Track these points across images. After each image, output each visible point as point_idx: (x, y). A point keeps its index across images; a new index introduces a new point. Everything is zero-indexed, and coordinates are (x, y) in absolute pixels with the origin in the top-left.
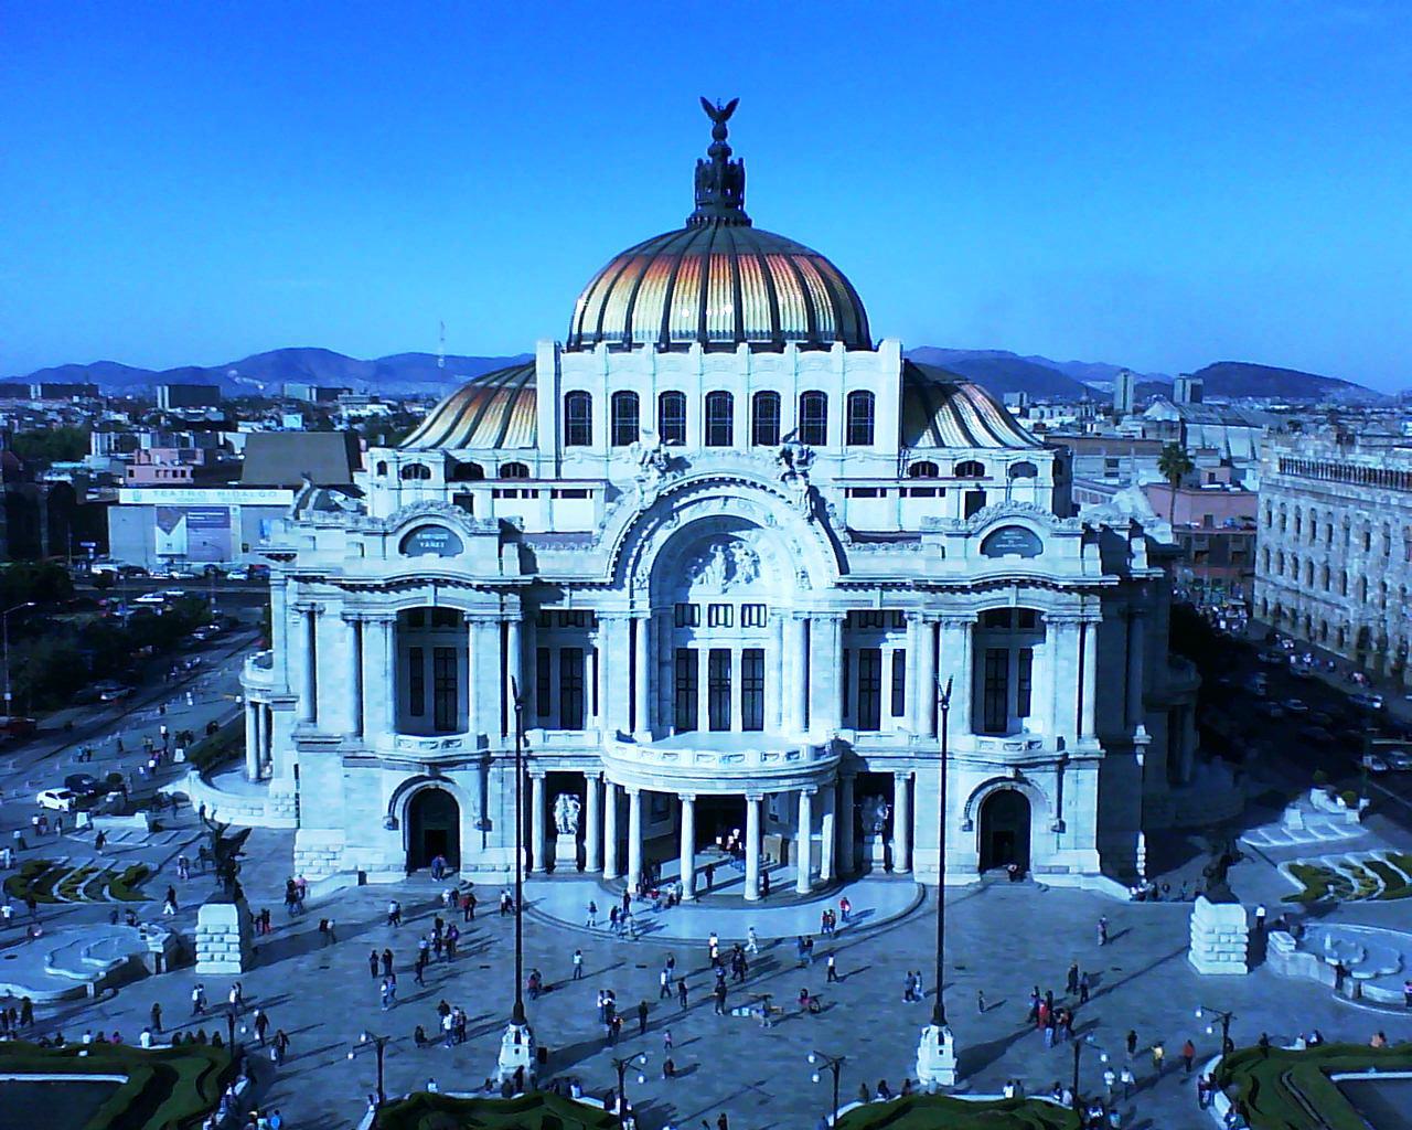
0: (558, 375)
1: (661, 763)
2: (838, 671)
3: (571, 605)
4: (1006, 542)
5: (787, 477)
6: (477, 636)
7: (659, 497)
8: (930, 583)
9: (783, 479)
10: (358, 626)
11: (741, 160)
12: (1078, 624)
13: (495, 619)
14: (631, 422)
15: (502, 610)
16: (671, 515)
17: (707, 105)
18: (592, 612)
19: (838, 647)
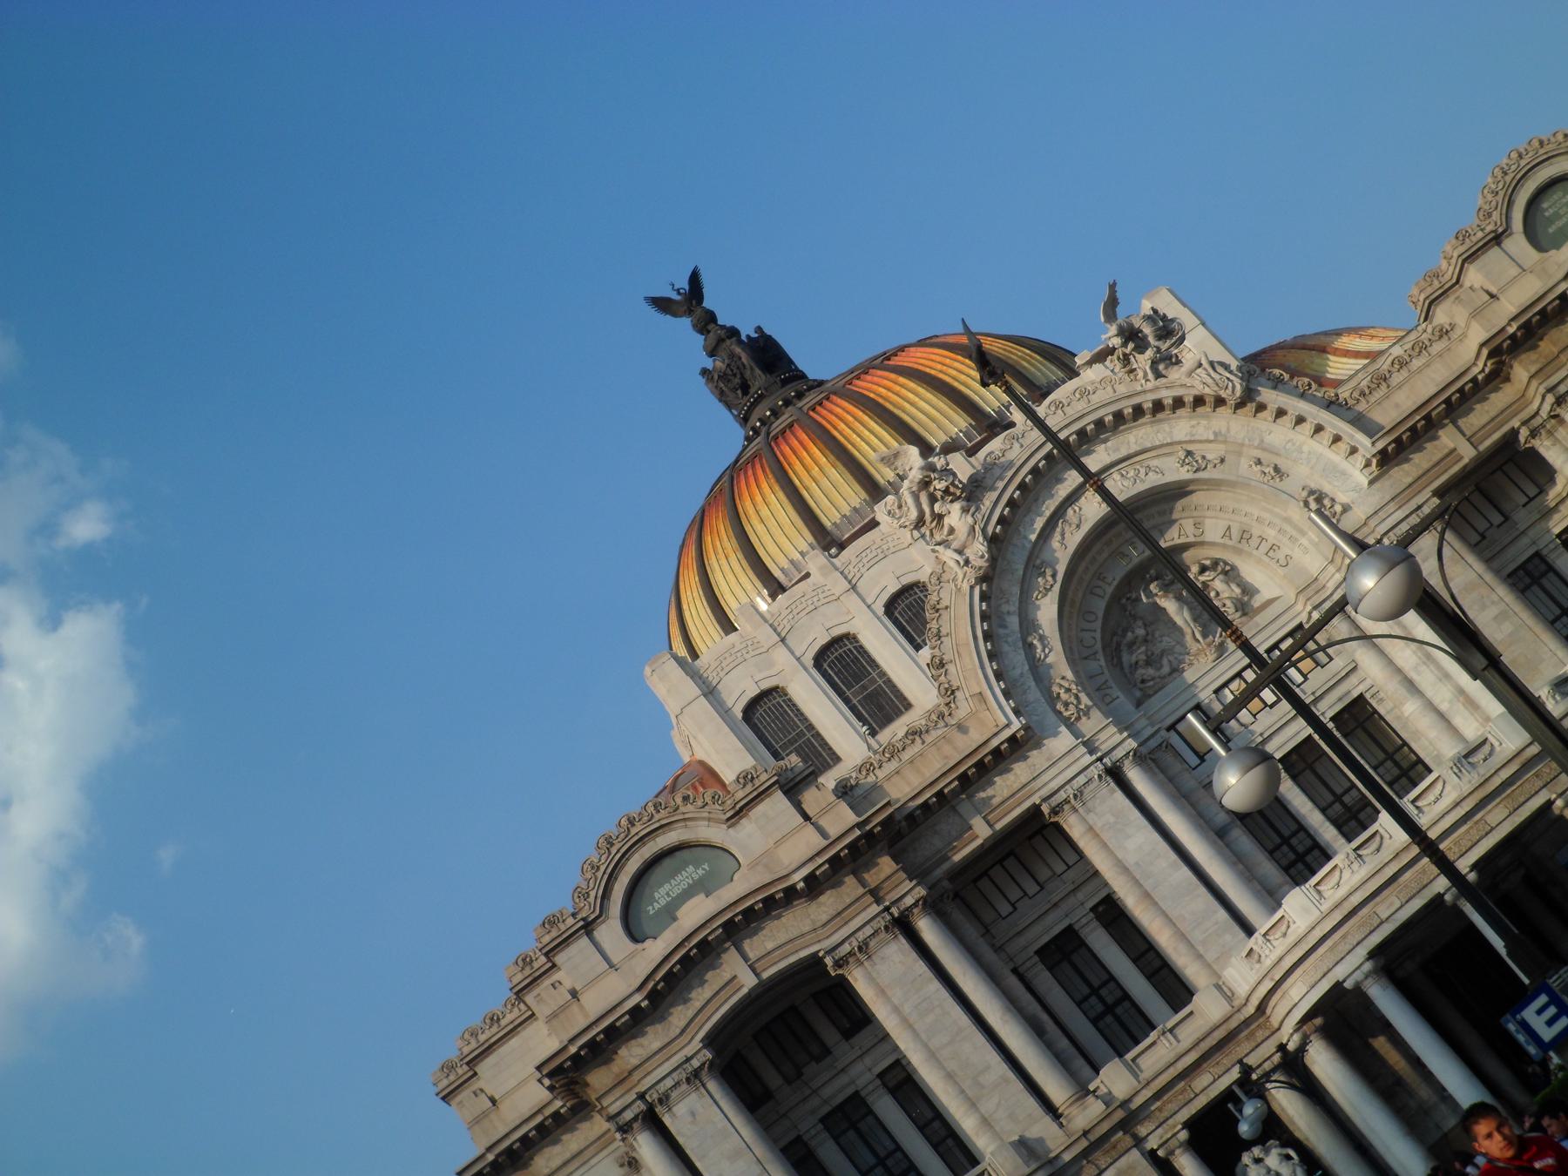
0: (710, 692)
1: (1362, 872)
2: (1502, 591)
4: (1557, 216)
5: (1161, 367)
6: (871, 979)
7: (993, 541)
8: (1511, 330)
9: (1158, 375)
10: (653, 1121)
11: (759, 329)
13: (880, 923)
14: (873, 681)
15: (878, 901)
16: (1036, 563)
17: (662, 305)
18: (1035, 811)
19: (1471, 559)
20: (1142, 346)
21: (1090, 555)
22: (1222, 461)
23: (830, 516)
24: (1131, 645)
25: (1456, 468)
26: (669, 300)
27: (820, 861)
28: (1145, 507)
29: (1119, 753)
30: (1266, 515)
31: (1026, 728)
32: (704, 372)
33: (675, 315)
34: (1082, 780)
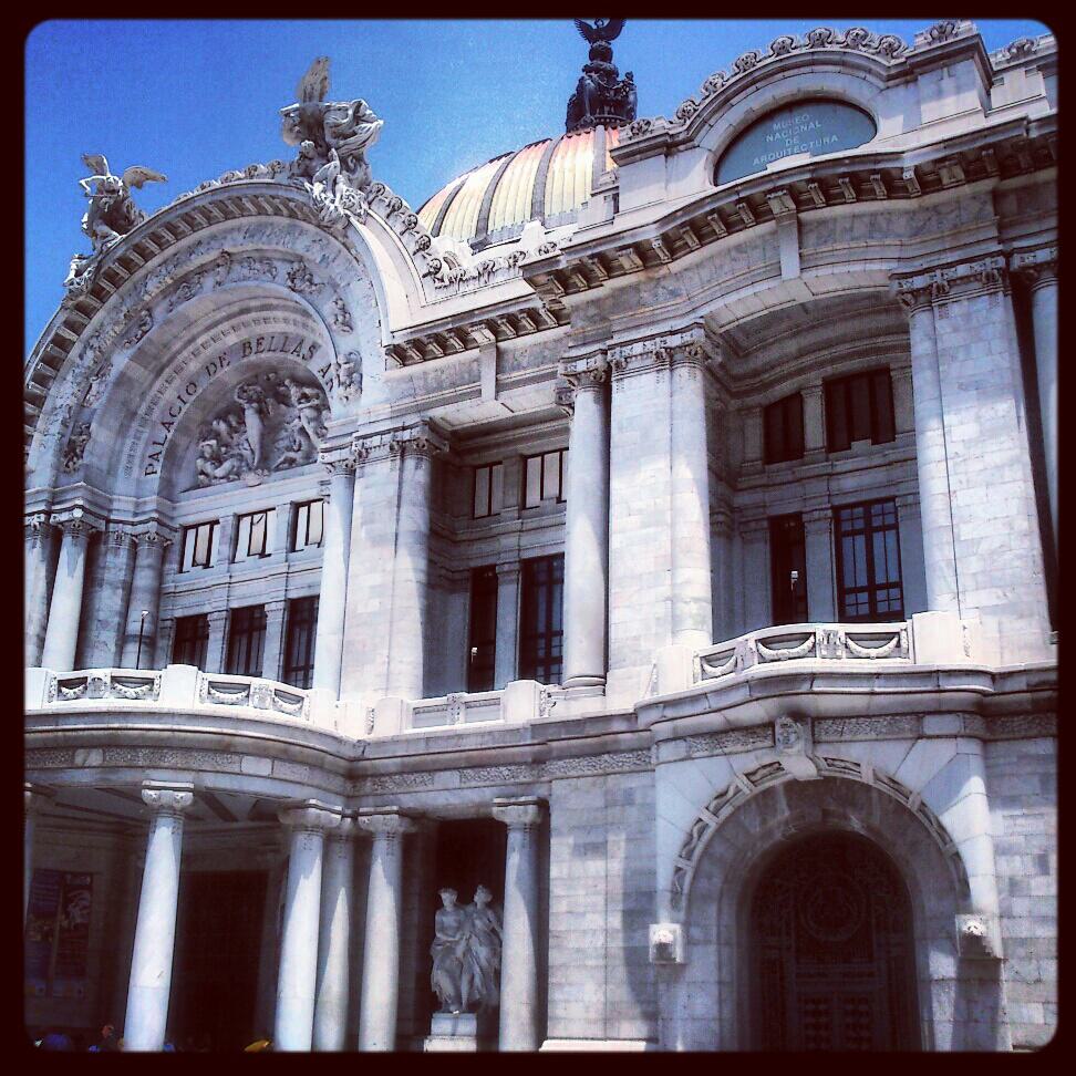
8: (561, 266)
12: (990, 278)
21: (212, 332)
28: (276, 308)
29: (64, 517)
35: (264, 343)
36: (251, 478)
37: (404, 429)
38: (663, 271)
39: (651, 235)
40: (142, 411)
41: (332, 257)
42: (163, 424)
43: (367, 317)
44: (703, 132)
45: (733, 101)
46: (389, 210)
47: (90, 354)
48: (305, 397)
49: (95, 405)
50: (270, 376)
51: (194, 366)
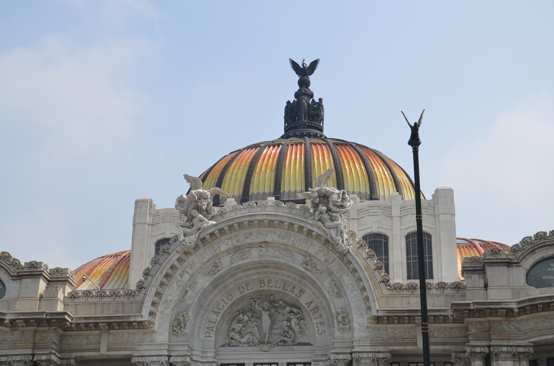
3: (108, 350)
8: (472, 307)
11: (320, 100)
13: (26, 358)
15: (33, 349)
17: (295, 65)
20: (327, 204)
22: (321, 273)
23: (254, 189)
24: (240, 321)
25: (409, 348)
26: (298, 65)
27: (21, 317)
28: (284, 269)
29: (179, 359)
30: (327, 308)
31: (150, 323)
32: (288, 102)
33: (297, 73)
34: (155, 359)
35: (272, 282)
36: (266, 347)
37: (378, 352)
38: (514, 319)
39: (514, 306)
40: (205, 305)
41: (330, 261)
42: (214, 312)
43: (352, 295)
44: (523, 261)
45: (536, 251)
46: (359, 246)
47: (187, 277)
48: (291, 312)
49: (189, 302)
50: (271, 297)
51: (232, 286)
